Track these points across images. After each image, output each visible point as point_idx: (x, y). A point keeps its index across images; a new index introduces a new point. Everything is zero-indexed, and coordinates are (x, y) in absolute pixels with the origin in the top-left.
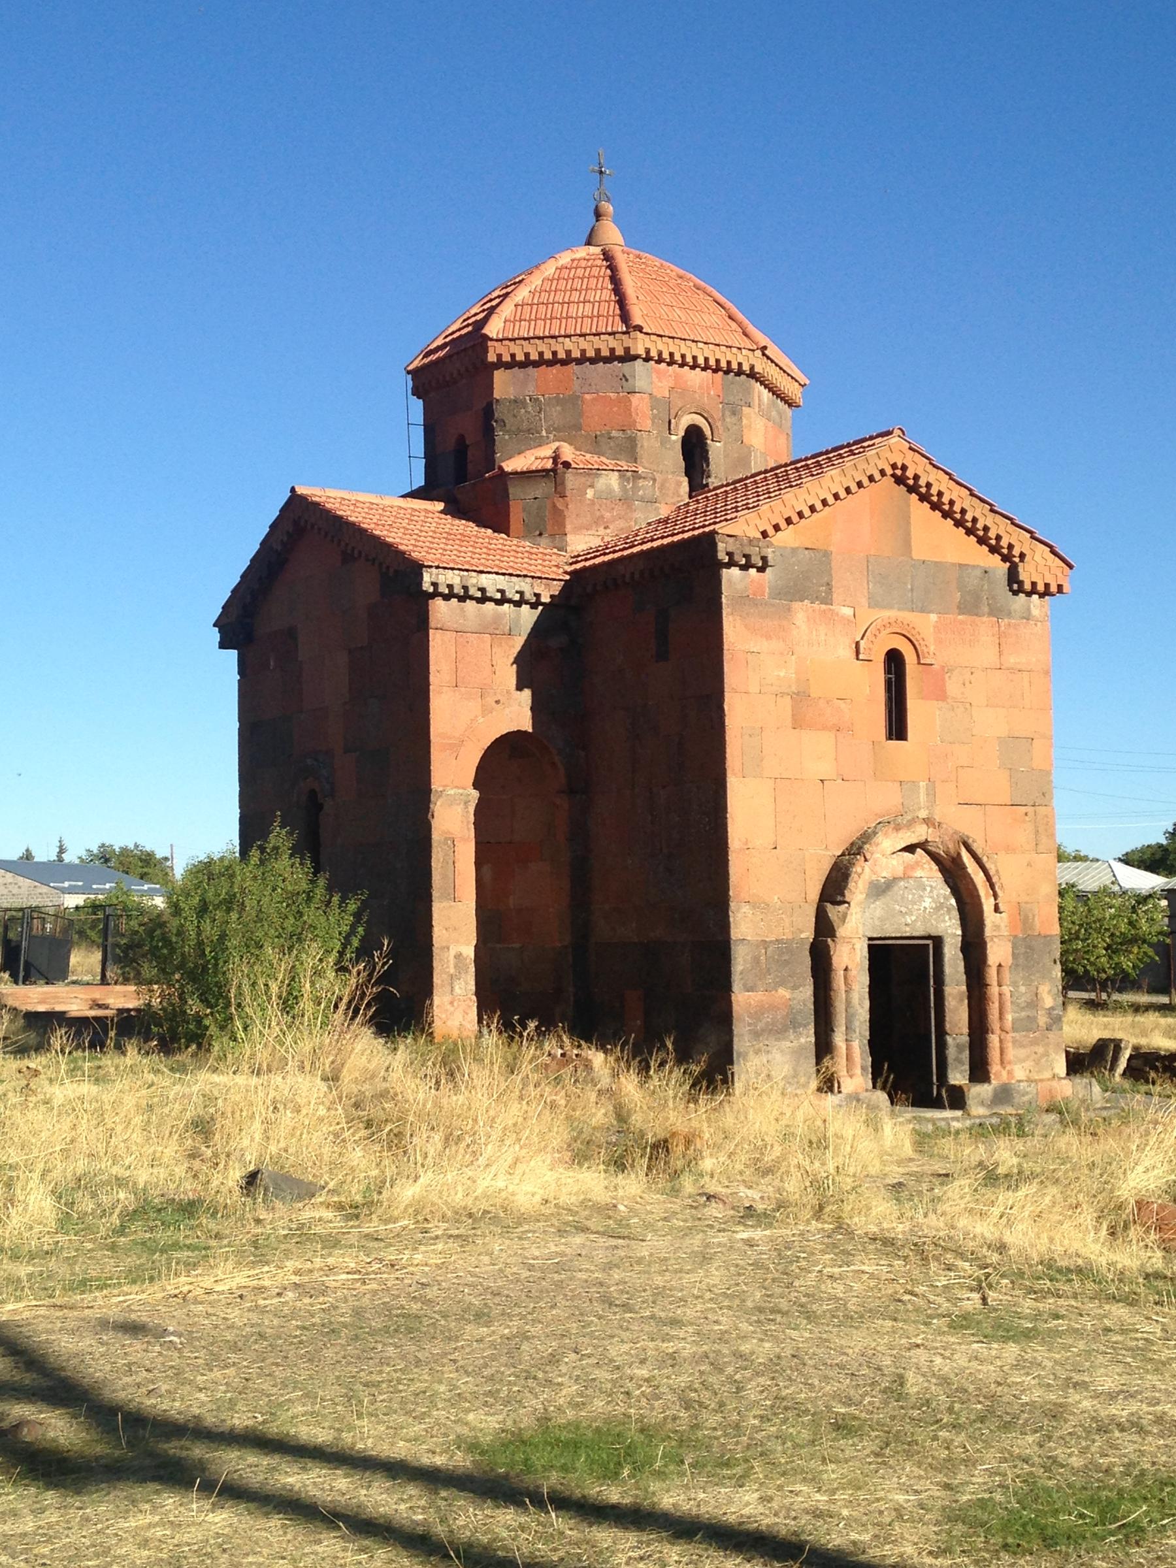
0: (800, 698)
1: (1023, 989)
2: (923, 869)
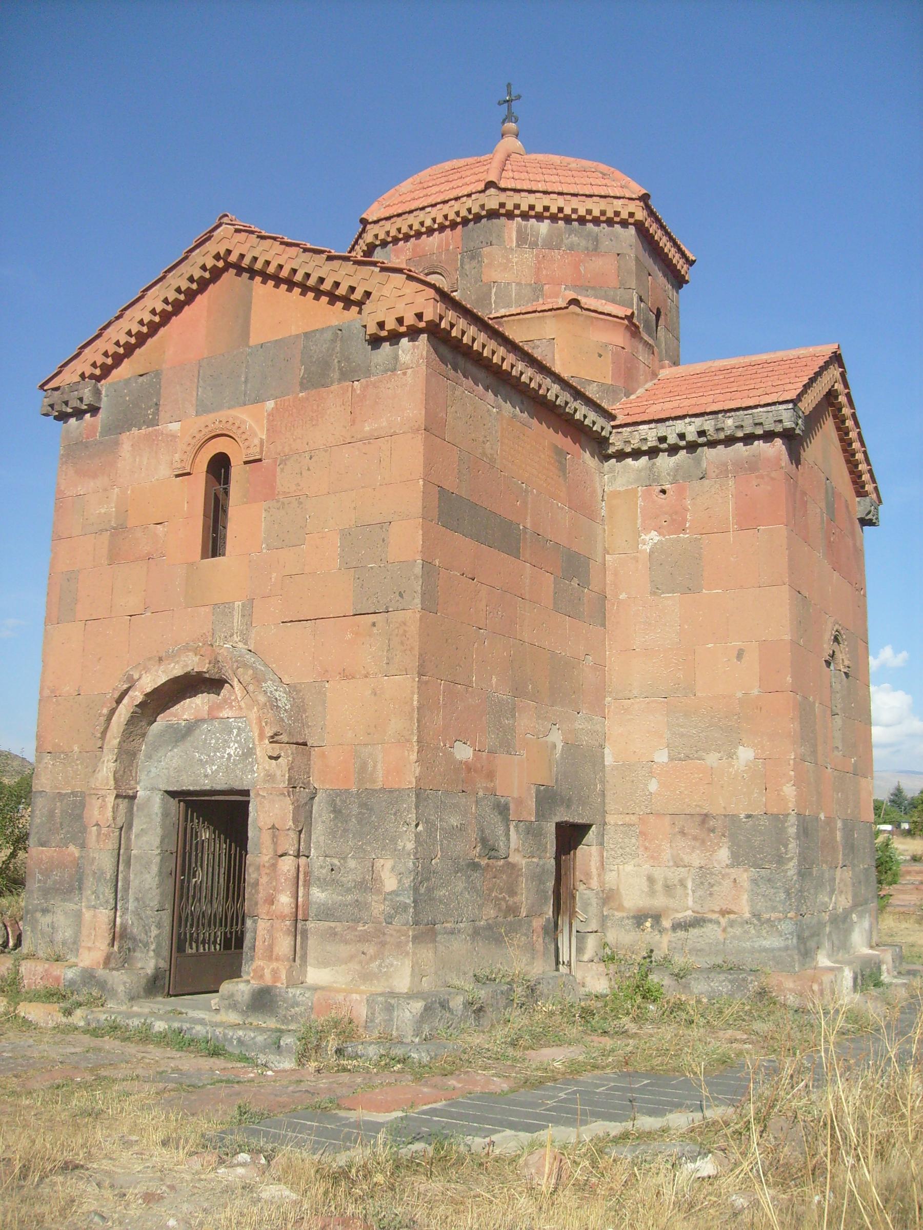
0: (119, 530)
1: (352, 864)
2: (231, 707)
